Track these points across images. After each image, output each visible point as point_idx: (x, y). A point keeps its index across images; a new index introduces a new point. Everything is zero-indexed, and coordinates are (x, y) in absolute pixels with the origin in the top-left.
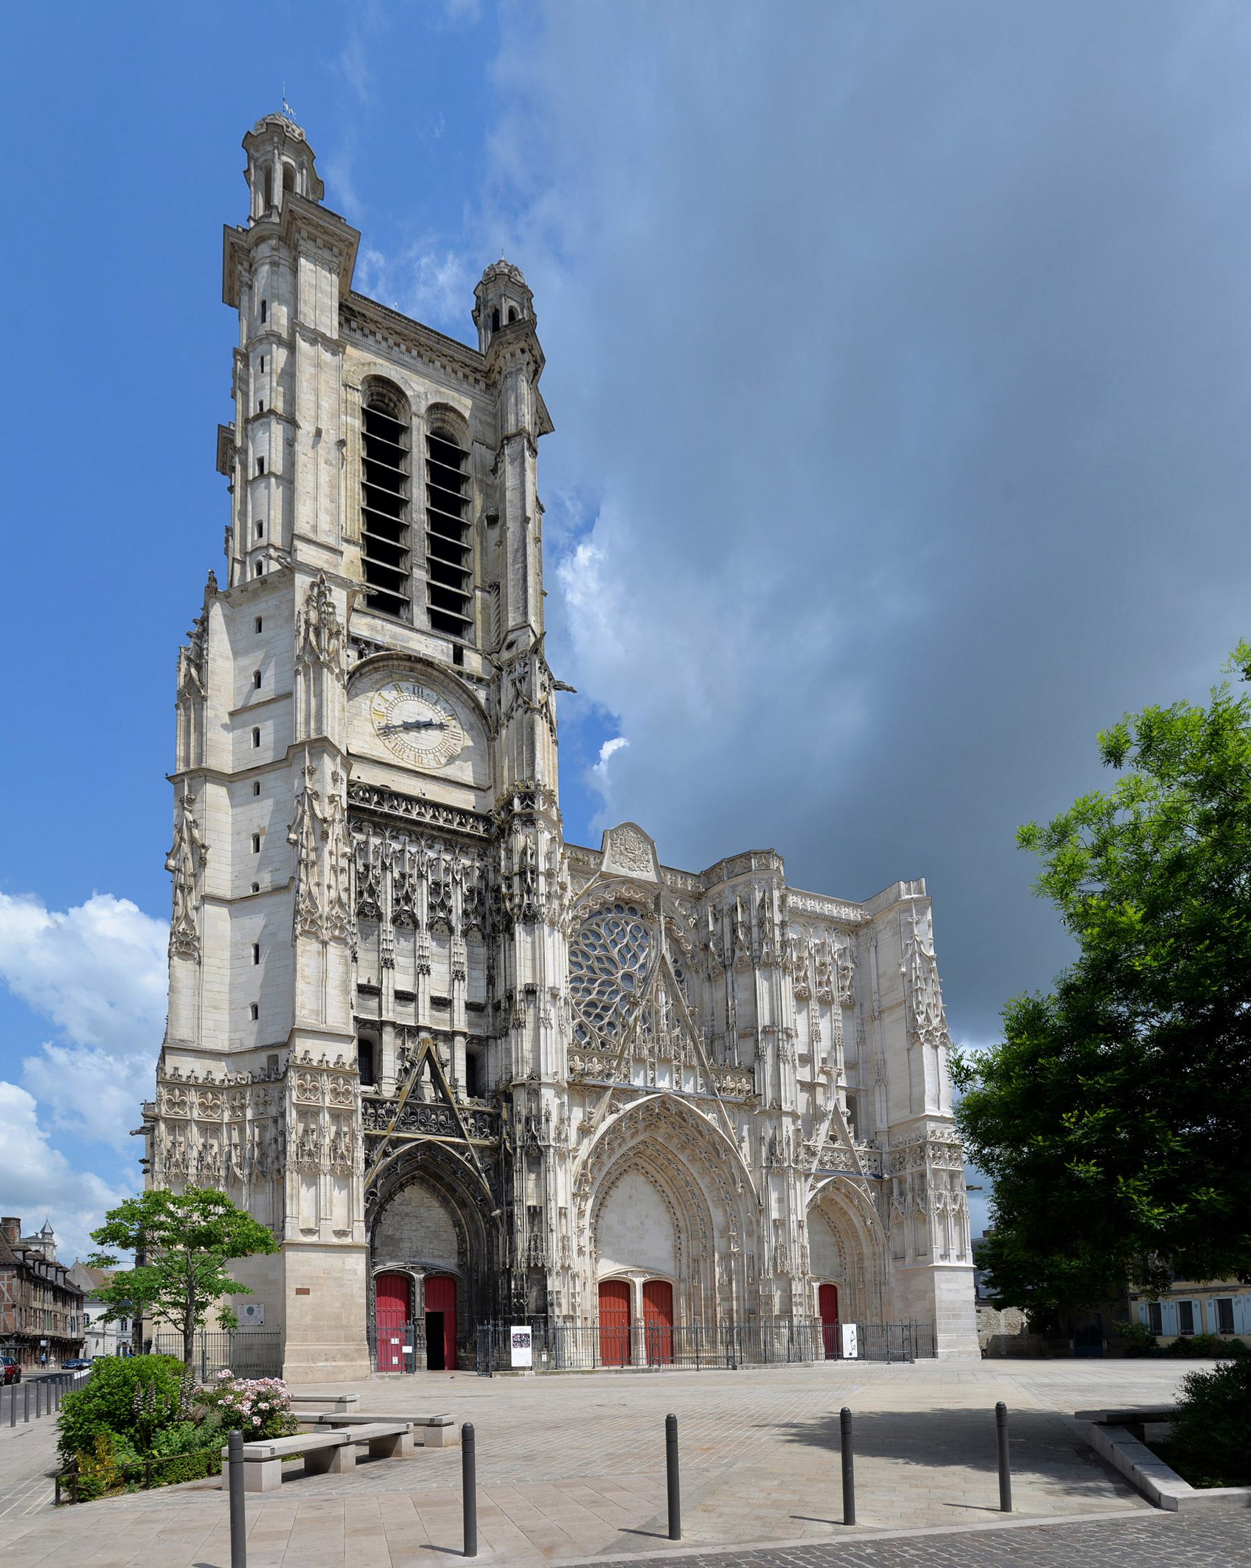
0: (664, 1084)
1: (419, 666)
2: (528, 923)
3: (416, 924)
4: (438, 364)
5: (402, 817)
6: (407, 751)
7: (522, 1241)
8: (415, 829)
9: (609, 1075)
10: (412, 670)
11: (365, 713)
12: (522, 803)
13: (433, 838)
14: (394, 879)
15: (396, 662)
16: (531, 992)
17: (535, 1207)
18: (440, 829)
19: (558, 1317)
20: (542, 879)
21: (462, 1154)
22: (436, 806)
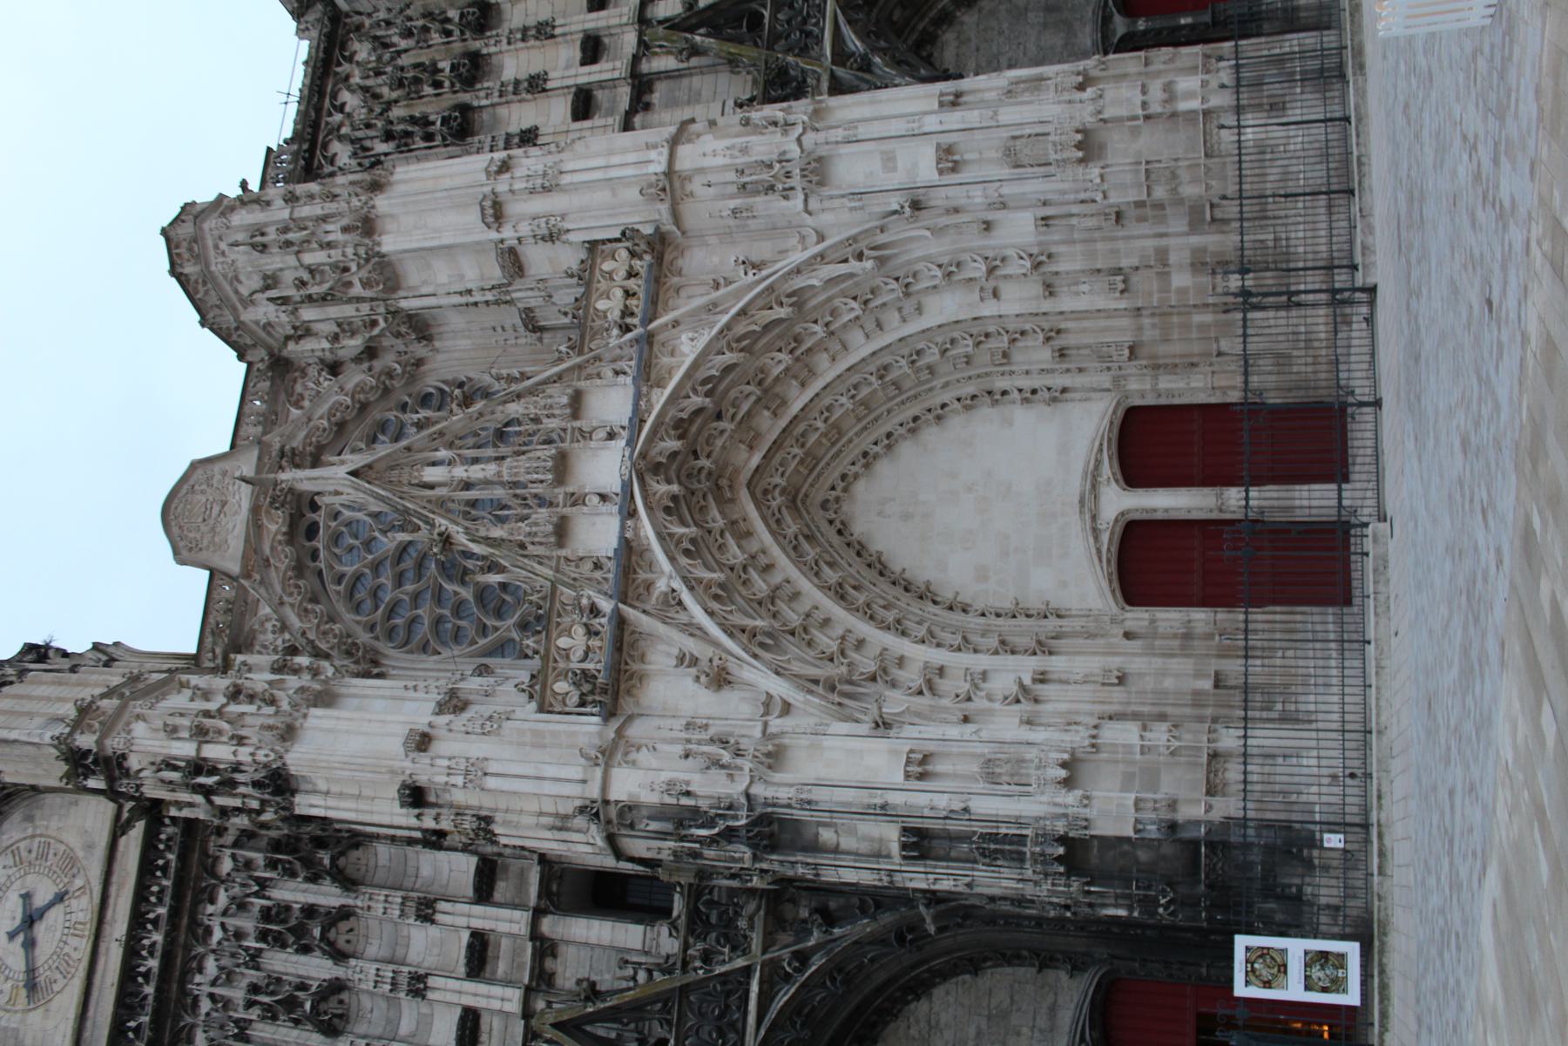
2: (294, 785)
3: (336, 987)
6: (67, 949)
7: (995, 881)
8: (179, 961)
9: (594, 611)
12: (94, 773)
13: (194, 922)
14: (263, 1018)
16: (415, 796)
17: (904, 846)
18: (175, 913)
19: (1209, 808)
20: (212, 752)
21: (787, 978)
22: (138, 920)
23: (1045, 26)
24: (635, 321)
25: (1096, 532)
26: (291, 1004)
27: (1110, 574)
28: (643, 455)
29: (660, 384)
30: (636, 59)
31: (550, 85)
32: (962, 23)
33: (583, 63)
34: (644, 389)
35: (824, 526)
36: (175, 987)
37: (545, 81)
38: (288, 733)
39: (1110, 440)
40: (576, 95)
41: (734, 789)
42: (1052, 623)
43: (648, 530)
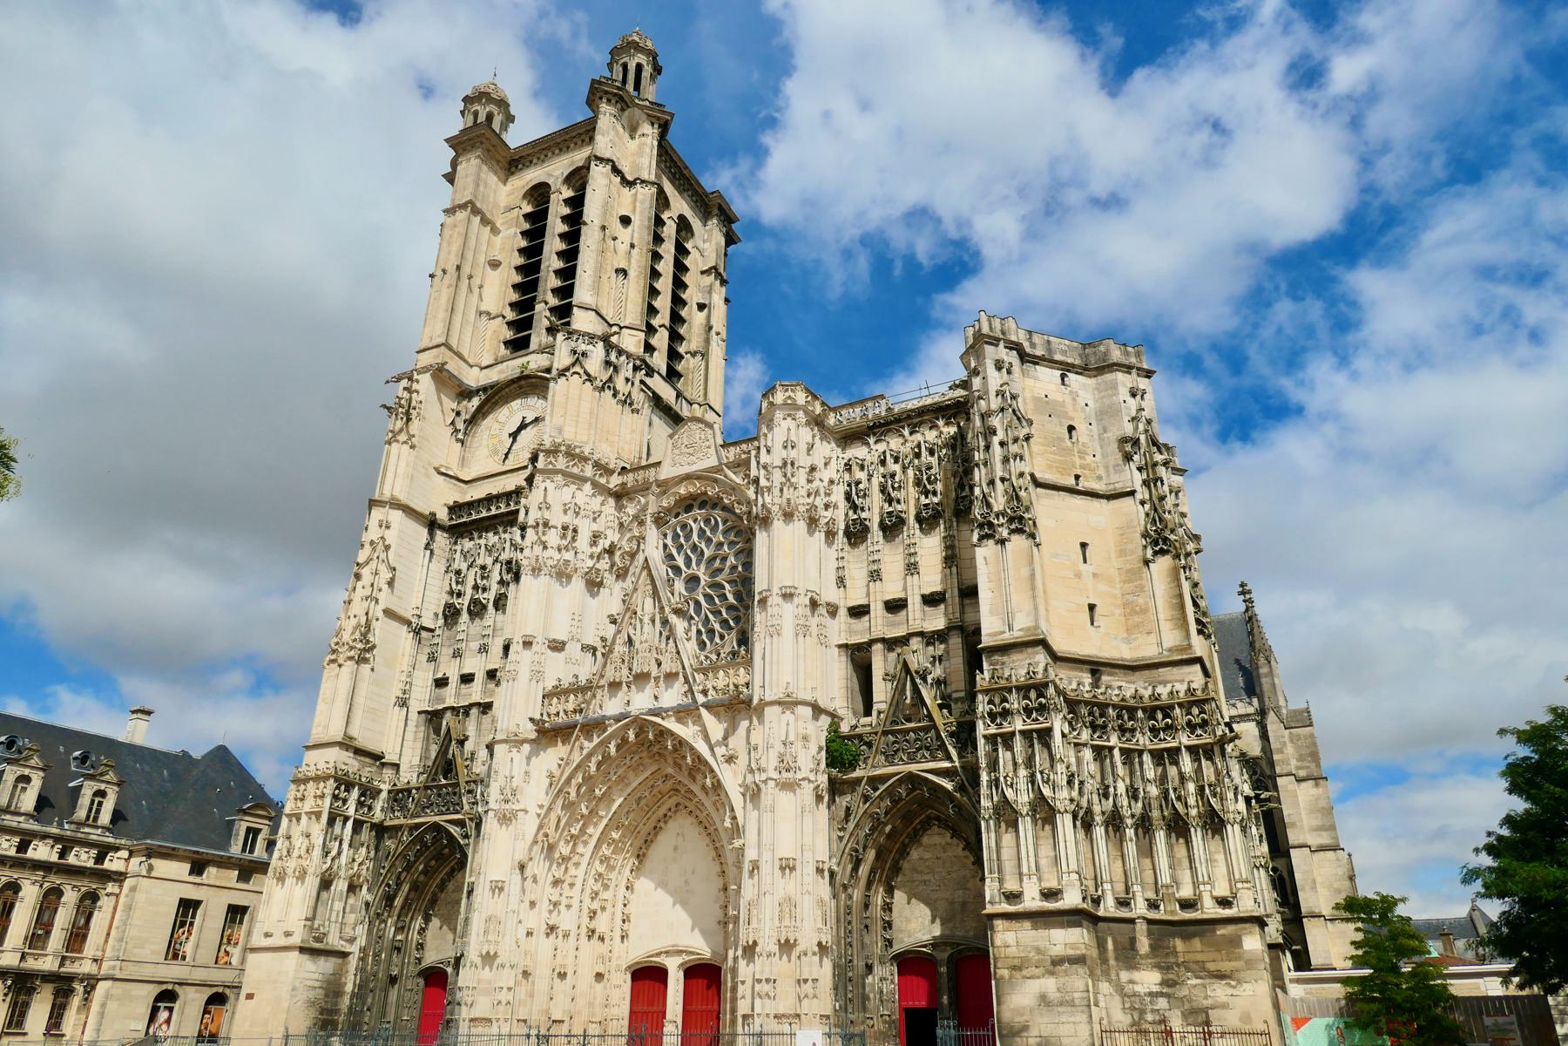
0: (641, 701)
1: (523, 382)
4: (572, 145)
5: (484, 518)
10: (521, 387)
11: (485, 442)
15: (507, 390)
20: (530, 532)
23: (952, 903)
24: (710, 697)
25: (658, 955)
26: (476, 587)
27: (641, 963)
28: (645, 720)
29: (679, 720)
30: (921, 634)
31: (909, 577)
32: (958, 846)
33: (923, 596)
34: (671, 713)
35: (668, 807)
36: (488, 523)
37: (912, 574)
38: (536, 571)
39: (700, 959)
40: (900, 599)
41: (492, 805)
42: (618, 933)
43: (610, 730)
